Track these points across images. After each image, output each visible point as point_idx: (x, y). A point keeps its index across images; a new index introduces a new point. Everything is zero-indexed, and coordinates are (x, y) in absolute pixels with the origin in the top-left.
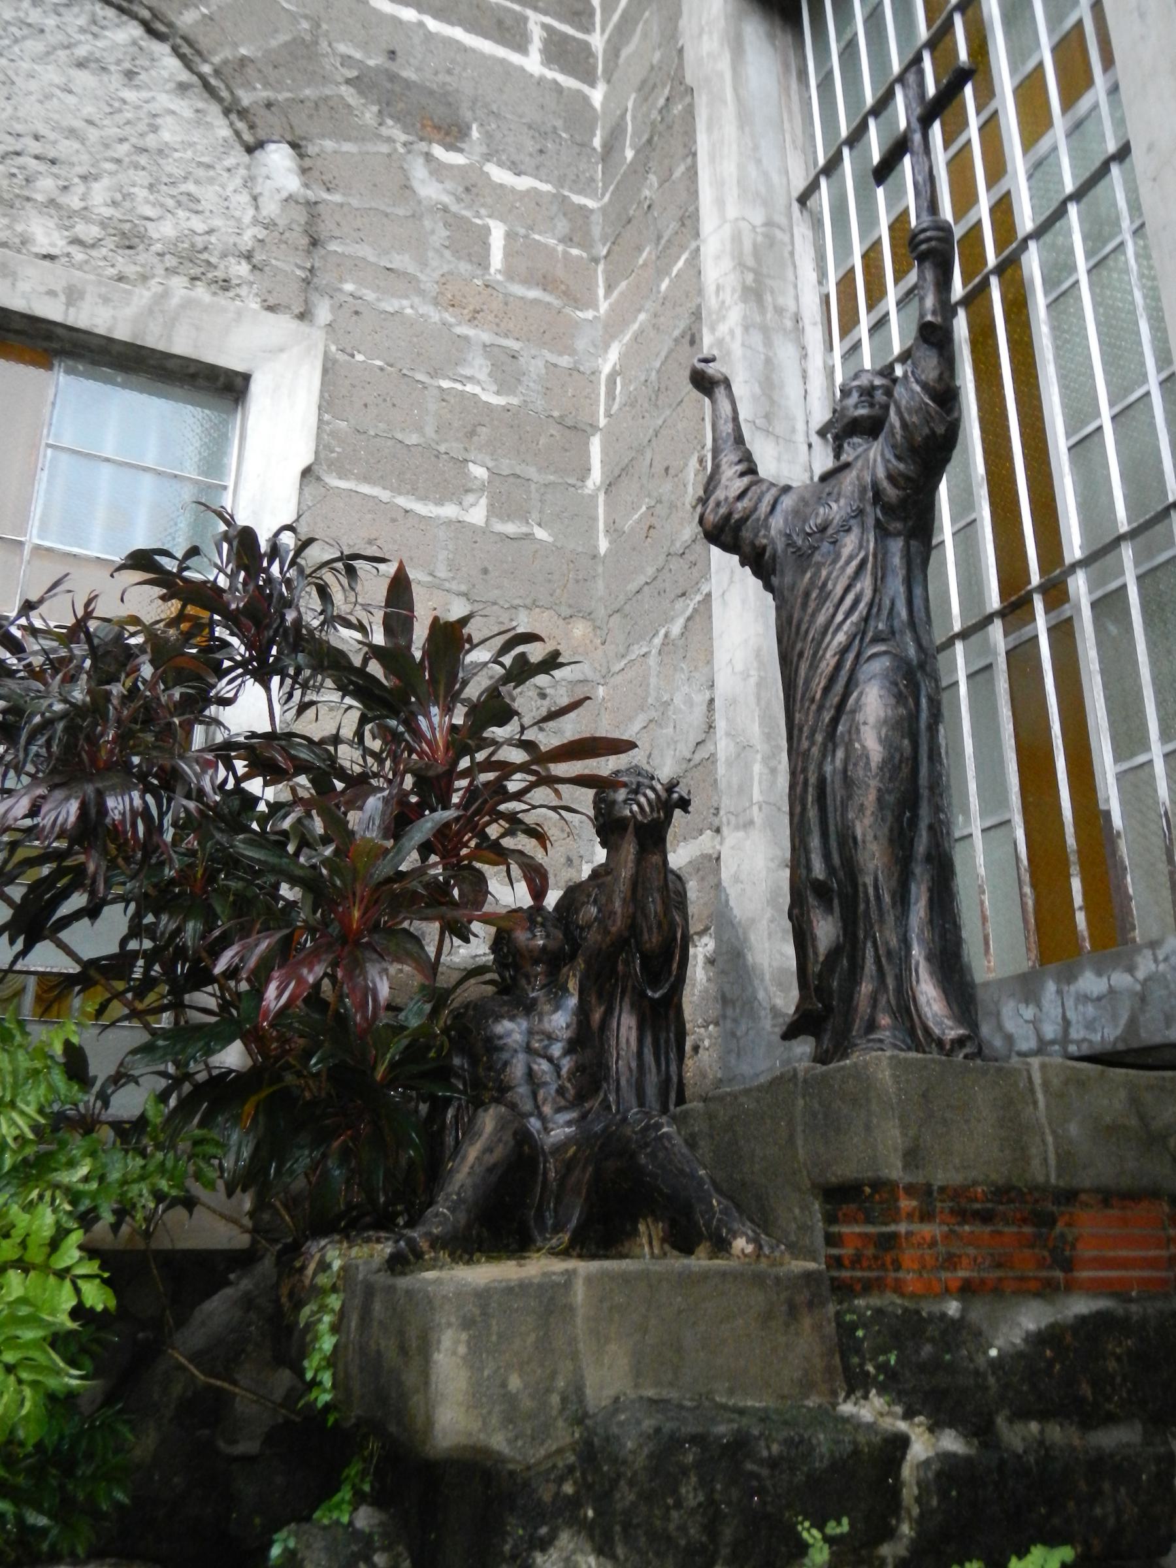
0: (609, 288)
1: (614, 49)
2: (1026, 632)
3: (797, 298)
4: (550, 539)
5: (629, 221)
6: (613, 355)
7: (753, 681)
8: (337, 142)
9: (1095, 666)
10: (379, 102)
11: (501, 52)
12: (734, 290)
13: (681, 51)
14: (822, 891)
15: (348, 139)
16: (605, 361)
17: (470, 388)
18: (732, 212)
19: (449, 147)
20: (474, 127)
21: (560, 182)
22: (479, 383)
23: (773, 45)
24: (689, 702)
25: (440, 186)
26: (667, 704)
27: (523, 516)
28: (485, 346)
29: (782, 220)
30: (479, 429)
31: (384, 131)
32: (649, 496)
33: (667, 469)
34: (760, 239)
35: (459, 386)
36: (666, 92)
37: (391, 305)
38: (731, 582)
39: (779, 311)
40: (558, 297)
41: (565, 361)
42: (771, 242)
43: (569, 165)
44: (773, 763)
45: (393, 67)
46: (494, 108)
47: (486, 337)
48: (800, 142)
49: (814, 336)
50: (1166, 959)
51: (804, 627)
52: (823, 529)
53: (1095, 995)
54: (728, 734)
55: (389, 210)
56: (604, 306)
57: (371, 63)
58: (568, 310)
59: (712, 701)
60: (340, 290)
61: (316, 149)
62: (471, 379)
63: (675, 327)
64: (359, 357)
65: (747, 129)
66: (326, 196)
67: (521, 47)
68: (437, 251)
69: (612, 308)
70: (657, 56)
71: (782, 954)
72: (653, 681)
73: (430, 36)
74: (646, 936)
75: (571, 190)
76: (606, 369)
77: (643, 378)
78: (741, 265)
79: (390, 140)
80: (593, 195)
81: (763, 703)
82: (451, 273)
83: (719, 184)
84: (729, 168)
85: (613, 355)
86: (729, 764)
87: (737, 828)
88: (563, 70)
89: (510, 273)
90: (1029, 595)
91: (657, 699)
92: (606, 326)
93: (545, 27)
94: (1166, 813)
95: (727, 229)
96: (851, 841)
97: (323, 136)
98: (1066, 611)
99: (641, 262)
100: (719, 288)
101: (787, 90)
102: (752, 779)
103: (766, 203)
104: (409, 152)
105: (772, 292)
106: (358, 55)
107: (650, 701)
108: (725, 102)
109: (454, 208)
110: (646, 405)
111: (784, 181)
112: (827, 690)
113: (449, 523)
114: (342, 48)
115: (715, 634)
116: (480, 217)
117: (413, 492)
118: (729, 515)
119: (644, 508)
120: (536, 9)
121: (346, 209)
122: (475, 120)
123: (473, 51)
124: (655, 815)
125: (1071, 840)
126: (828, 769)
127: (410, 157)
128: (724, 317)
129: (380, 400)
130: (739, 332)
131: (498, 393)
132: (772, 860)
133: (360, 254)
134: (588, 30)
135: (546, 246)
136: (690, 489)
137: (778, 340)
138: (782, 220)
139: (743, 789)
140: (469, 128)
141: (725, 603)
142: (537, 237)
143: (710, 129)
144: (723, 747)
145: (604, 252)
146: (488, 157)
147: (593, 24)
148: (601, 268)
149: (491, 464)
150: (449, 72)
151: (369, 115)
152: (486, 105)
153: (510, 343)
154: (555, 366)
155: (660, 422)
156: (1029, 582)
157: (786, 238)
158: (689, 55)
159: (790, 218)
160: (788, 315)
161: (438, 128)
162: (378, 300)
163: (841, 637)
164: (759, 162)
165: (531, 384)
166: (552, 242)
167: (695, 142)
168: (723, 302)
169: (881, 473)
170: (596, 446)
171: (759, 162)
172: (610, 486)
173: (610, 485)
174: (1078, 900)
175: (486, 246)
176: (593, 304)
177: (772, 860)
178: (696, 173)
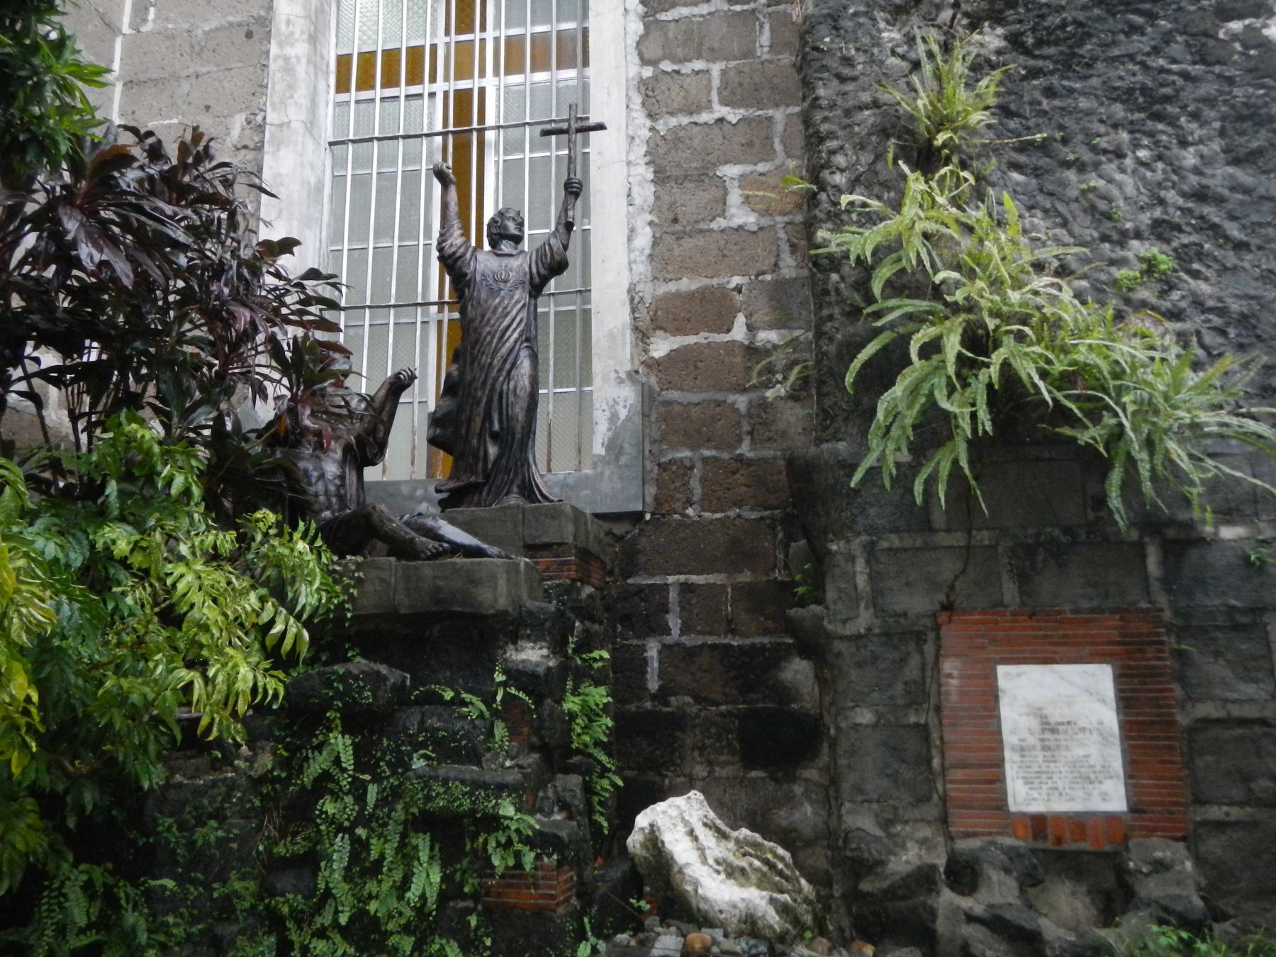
12: (302, 32)
14: (495, 437)
32: (183, 115)
33: (208, 108)
39: (322, 57)
42: (323, 11)
51: (492, 322)
52: (506, 282)
77: (186, 26)
78: (307, 17)
100: (288, 22)
110: (186, 48)
112: (509, 354)
118: (454, 253)
119: (175, 121)
126: (505, 388)
128: (292, 45)
130: (304, 61)
155: (204, 70)
163: (516, 335)
168: (292, 34)
169: (534, 270)
173: (131, 82)
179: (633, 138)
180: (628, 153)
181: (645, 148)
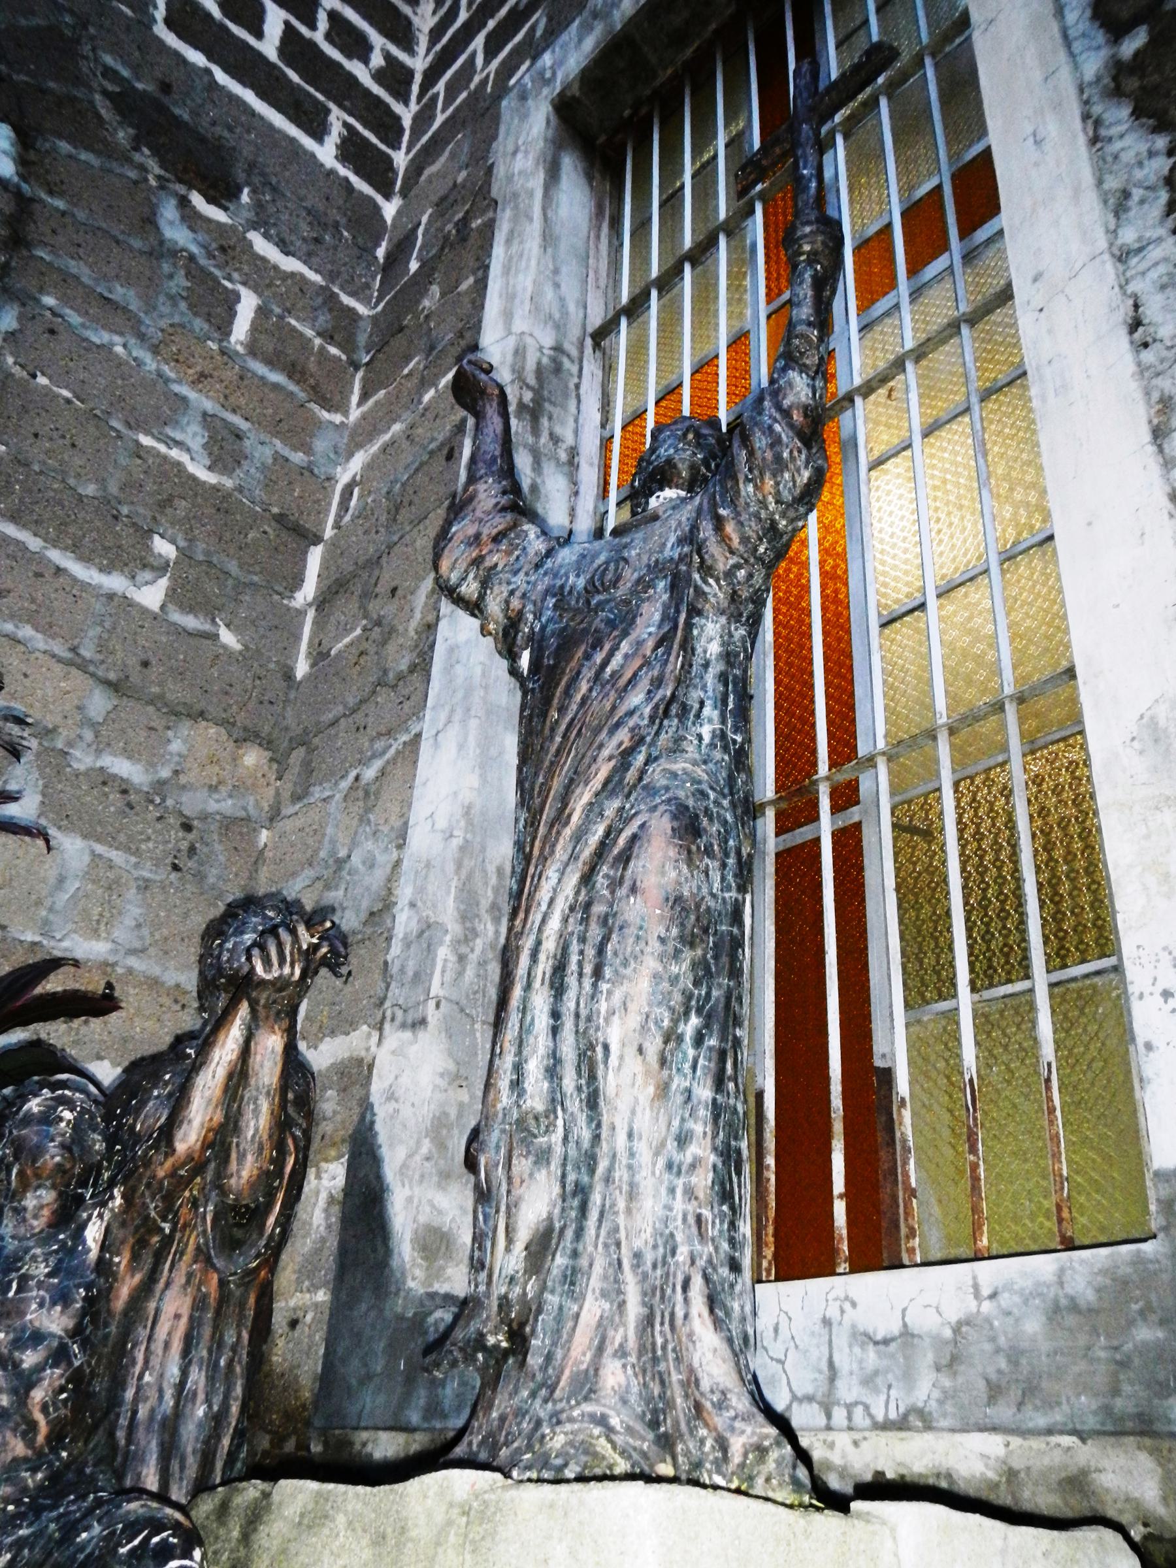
0: (365, 396)
1: (416, 168)
2: (802, 835)
3: (576, 432)
4: (238, 647)
5: (401, 329)
6: (357, 463)
7: (456, 843)
8: (75, 147)
9: (890, 882)
10: (137, 127)
11: (293, 131)
13: (490, 170)
15: (89, 148)
16: (345, 471)
17: (175, 453)
18: (520, 324)
19: (210, 200)
20: (246, 191)
21: (332, 276)
22: (188, 450)
23: (591, 186)
24: (371, 864)
25: (191, 235)
26: (341, 863)
27: (210, 610)
28: (205, 414)
29: (574, 352)
30: (176, 502)
31: (137, 157)
33: (394, 591)
34: (545, 360)
35: (162, 448)
36: (467, 207)
37: (100, 337)
38: (449, 721)
39: (555, 439)
40: (303, 390)
41: (298, 458)
42: (558, 369)
43: (345, 265)
44: (464, 949)
45: (165, 100)
46: (274, 180)
47: (209, 406)
48: (603, 282)
49: (589, 476)
50: (993, 1296)
53: (879, 1337)
54: (412, 905)
55: (121, 237)
56: (355, 414)
57: (140, 86)
58: (312, 406)
59: (398, 864)
60: (38, 301)
61: (47, 145)
62: (179, 444)
63: (433, 439)
64: (42, 380)
65: (549, 250)
66: (43, 196)
67: (319, 133)
68: (171, 297)
69: (364, 417)
70: (463, 174)
71: (433, 1206)
72: (329, 830)
73: (213, 85)
74: (233, 1166)
75: (342, 288)
76: (344, 478)
79: (143, 168)
80: (366, 301)
81: (464, 873)
82: (182, 325)
83: (510, 297)
84: (525, 282)
85: (357, 463)
86: (408, 945)
87: (403, 1026)
88: (357, 173)
89: (253, 348)
90: (815, 783)
91: (333, 853)
92: (352, 436)
93: (346, 125)
94: (971, 1080)
95: (511, 342)
96: (599, 1049)
97: (61, 136)
98: (854, 814)
99: (406, 371)
101: (599, 228)
102: (433, 965)
103: (559, 327)
104: (162, 187)
105: (550, 418)
106: (125, 73)
107: (322, 854)
108: (531, 220)
109: (203, 261)
111: (581, 315)
113: (111, 596)
114: (108, 59)
115: (418, 780)
116: (230, 279)
117: (76, 549)
119: (358, 631)
120: (341, 106)
121: (68, 220)
122: (248, 184)
123: (261, 118)
124: (287, 970)
125: (837, 1101)
127: (162, 193)
129: (55, 435)
131: (210, 468)
132: (442, 1075)
133: (74, 271)
134: (396, 146)
135: (301, 335)
136: (418, 615)
137: (548, 468)
138: (574, 352)
139: (420, 978)
140: (240, 191)
141: (436, 745)
142: (293, 322)
143: (509, 241)
144: (404, 921)
145: (366, 359)
146: (255, 226)
147: (400, 143)
148: (360, 375)
149: (182, 544)
150: (231, 129)
151: (123, 136)
152: (263, 174)
153: (236, 420)
154: (287, 460)
156: (816, 772)
157: (575, 369)
158: (500, 171)
159: (582, 352)
160: (564, 446)
161: (204, 178)
162: (83, 325)
164: (557, 286)
165: (253, 470)
166: (309, 333)
167: (490, 256)
170: (315, 557)
171: (557, 286)
172: (322, 603)
174: (839, 1184)
175: (232, 314)
176: (343, 409)
177: (442, 1075)
178: (486, 287)
179: (1126, 194)
180: (1114, 233)
181: (1164, 196)
